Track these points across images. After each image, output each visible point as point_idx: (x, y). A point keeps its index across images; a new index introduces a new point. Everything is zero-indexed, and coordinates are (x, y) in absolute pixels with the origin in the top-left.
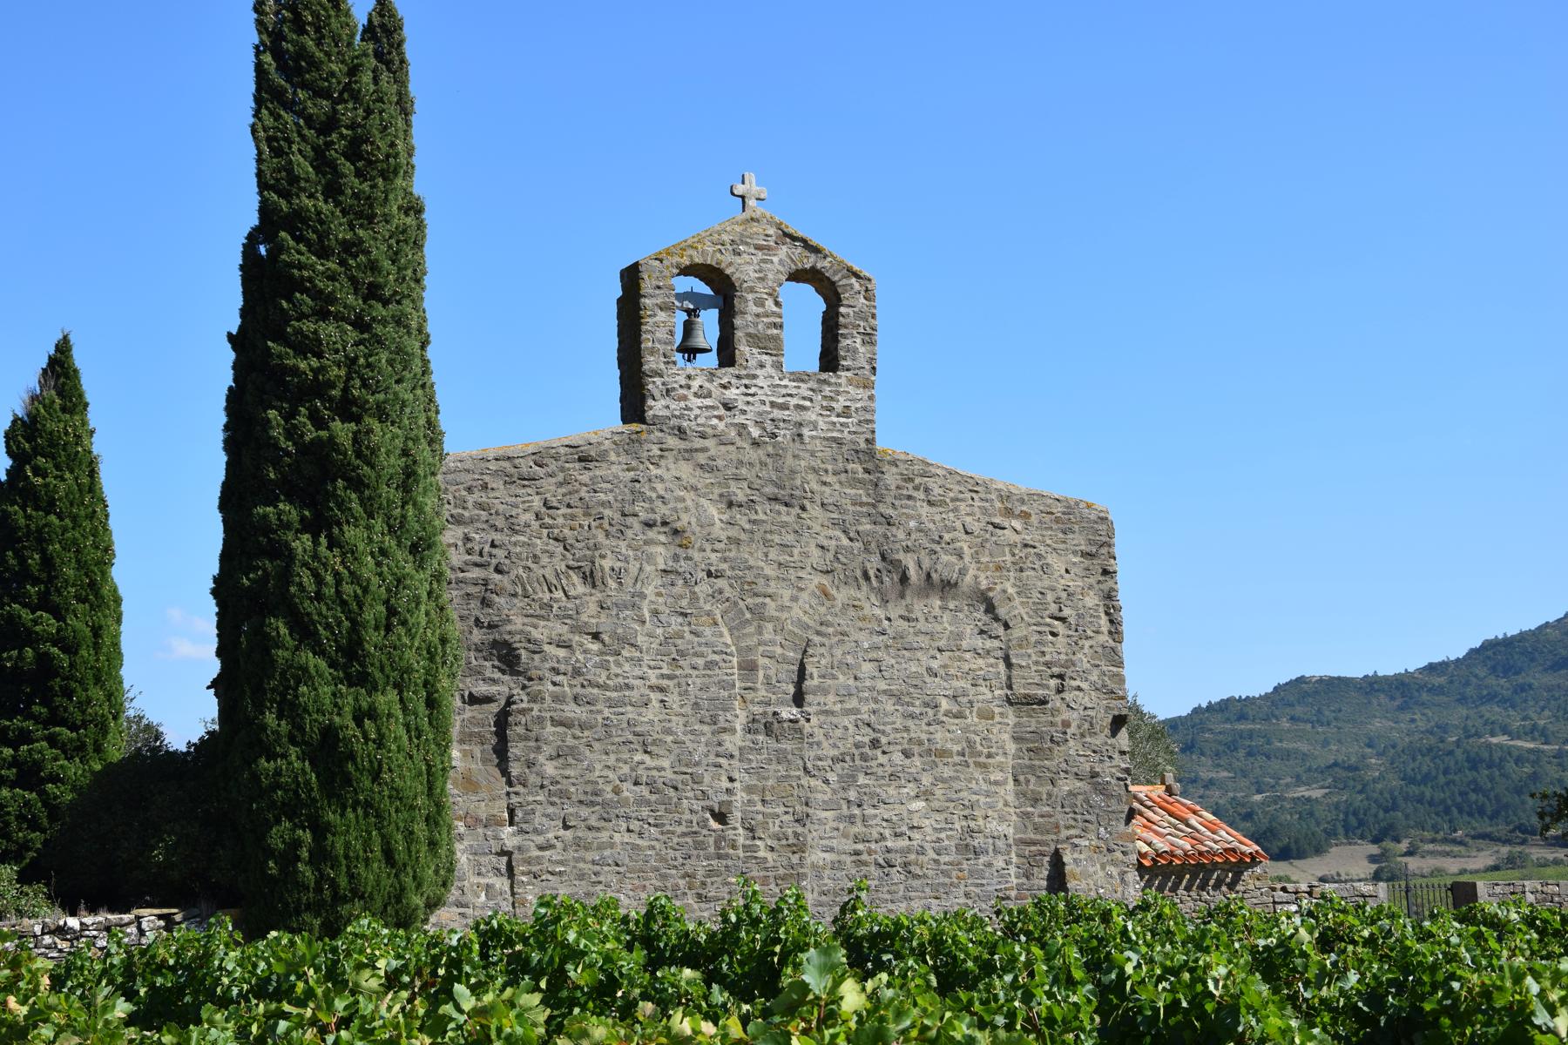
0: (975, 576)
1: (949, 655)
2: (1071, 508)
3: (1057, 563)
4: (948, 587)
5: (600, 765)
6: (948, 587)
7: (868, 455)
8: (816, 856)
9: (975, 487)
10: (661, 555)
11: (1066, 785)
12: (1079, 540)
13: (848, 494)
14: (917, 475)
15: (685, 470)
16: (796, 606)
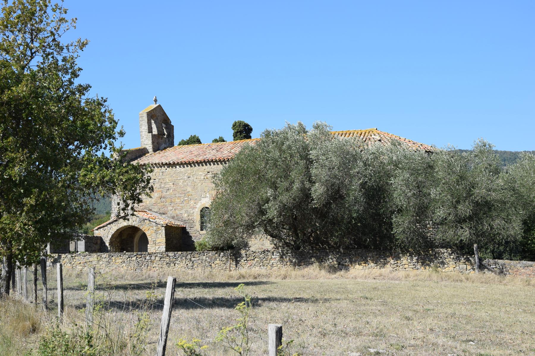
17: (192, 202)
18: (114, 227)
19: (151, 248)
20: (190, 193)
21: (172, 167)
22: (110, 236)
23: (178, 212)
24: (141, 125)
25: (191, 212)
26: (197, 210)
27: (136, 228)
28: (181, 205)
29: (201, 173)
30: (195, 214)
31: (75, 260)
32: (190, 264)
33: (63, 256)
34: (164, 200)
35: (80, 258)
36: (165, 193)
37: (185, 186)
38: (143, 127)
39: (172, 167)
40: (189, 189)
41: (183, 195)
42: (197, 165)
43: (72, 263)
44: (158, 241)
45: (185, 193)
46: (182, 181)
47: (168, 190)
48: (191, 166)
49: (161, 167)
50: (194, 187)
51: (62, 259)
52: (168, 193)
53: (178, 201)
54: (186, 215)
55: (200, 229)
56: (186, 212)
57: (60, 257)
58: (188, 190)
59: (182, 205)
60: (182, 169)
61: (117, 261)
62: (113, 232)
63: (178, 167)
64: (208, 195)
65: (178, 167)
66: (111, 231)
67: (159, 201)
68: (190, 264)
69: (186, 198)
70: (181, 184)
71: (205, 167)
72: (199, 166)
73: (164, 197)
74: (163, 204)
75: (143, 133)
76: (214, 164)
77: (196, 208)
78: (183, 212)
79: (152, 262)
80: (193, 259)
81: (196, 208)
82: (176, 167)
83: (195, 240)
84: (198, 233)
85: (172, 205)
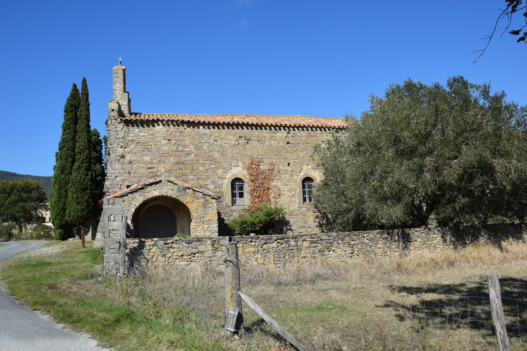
17: (220, 171)
18: (138, 198)
19: (197, 229)
20: (217, 160)
21: (194, 127)
22: (133, 210)
23: (202, 183)
24: (116, 82)
25: (220, 183)
26: (226, 181)
27: (174, 199)
28: (205, 174)
29: (232, 137)
30: (224, 185)
31: (172, 250)
32: (349, 250)
33: (149, 242)
34: (182, 166)
35: (181, 246)
36: (184, 158)
37: (211, 151)
38: (117, 85)
39: (194, 127)
40: (216, 155)
41: (209, 162)
42: (226, 127)
43: (169, 255)
44: (208, 218)
45: (211, 159)
46: (206, 145)
47: (188, 154)
48: (219, 128)
49: (178, 125)
51: (147, 248)
52: (187, 159)
53: (201, 168)
54: (212, 186)
55: (231, 204)
56: (213, 182)
57: (142, 245)
58: (215, 156)
59: (207, 174)
60: (207, 131)
61: (246, 250)
62: (138, 205)
63: (201, 127)
64: (240, 164)
65: (201, 127)
66: (134, 203)
67: (176, 167)
68: (349, 250)
69: (213, 166)
70: (205, 148)
71: (236, 130)
72: (229, 128)
73: (182, 163)
74: (181, 171)
75: (118, 92)
76: (248, 129)
77: (225, 178)
78: (209, 182)
79: (299, 249)
80: (353, 243)
81: (225, 178)
82: (199, 128)
83: (224, 218)
84: (228, 209)
85: (194, 173)
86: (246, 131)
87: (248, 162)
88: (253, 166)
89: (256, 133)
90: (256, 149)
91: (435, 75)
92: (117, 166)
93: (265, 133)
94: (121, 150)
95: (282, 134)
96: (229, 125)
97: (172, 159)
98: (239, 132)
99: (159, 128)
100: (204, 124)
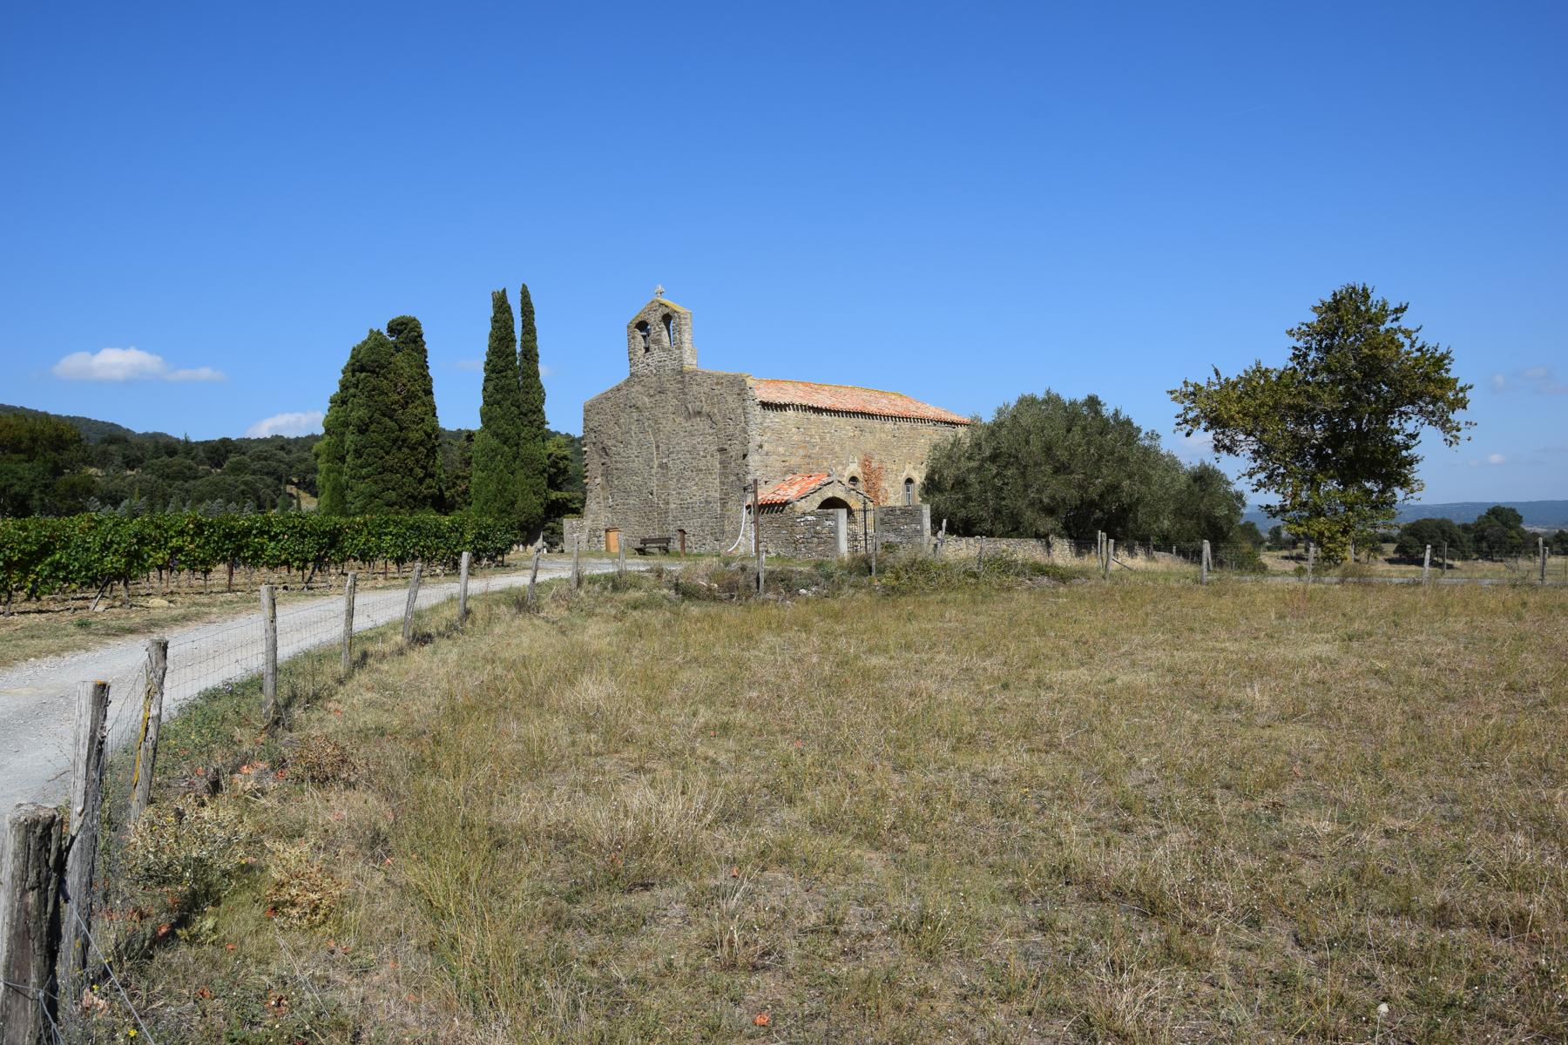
0: (706, 409)
1: (704, 439)
2: (735, 377)
3: (730, 399)
4: (699, 413)
5: (627, 481)
6: (699, 413)
7: (681, 372)
8: (672, 506)
9: (710, 376)
10: (635, 415)
11: (732, 478)
12: (736, 390)
13: (675, 386)
14: (695, 373)
15: (638, 388)
16: (667, 426)
40: (837, 448)
50: (842, 449)
86: (861, 420)
87: (862, 457)
88: (866, 463)
89: (869, 422)
90: (869, 443)
91: (1073, 392)
92: (757, 457)
93: (876, 423)
94: (759, 438)
95: (889, 425)
96: (848, 413)
97: (802, 452)
98: (854, 420)
99: (790, 413)
100: (828, 411)
